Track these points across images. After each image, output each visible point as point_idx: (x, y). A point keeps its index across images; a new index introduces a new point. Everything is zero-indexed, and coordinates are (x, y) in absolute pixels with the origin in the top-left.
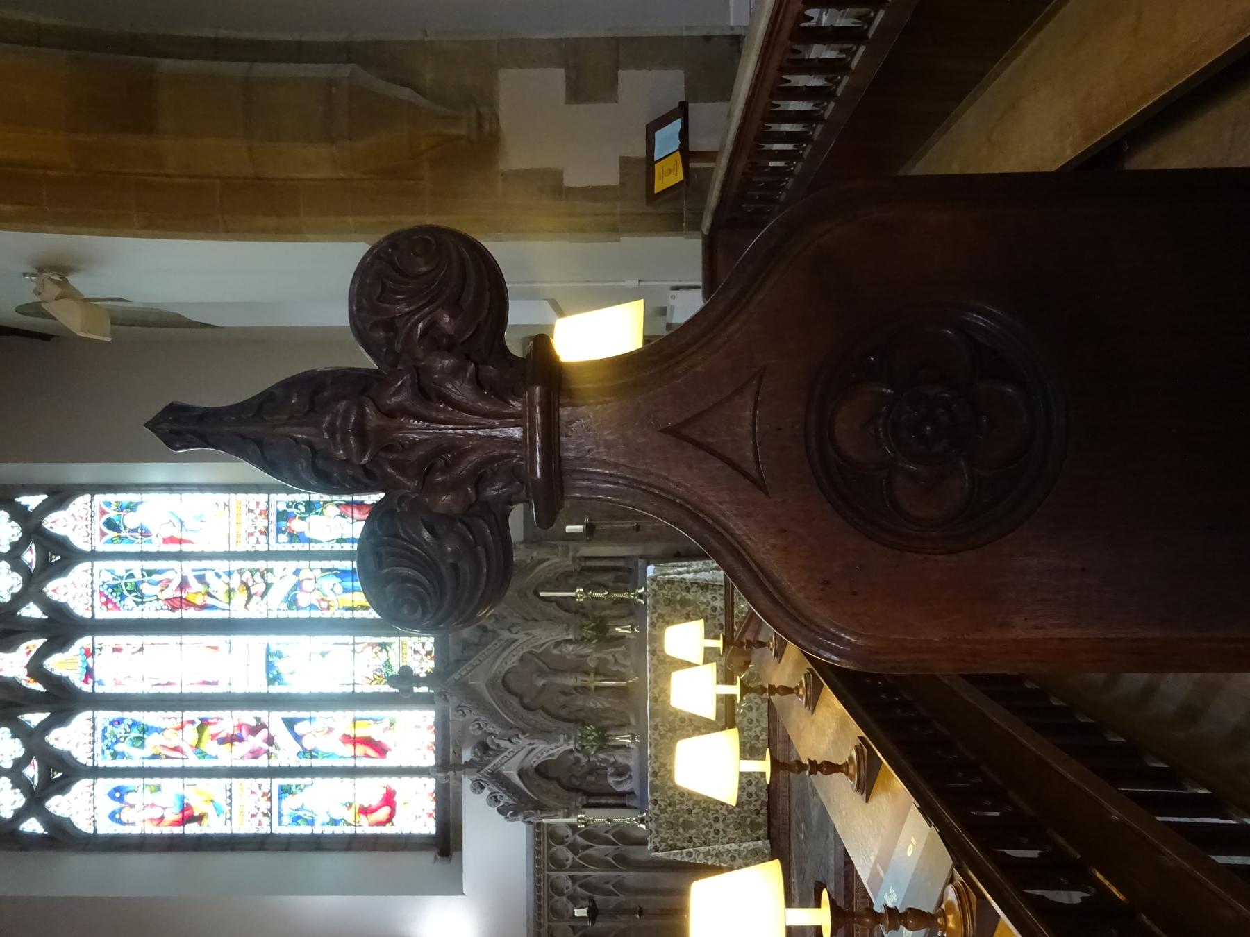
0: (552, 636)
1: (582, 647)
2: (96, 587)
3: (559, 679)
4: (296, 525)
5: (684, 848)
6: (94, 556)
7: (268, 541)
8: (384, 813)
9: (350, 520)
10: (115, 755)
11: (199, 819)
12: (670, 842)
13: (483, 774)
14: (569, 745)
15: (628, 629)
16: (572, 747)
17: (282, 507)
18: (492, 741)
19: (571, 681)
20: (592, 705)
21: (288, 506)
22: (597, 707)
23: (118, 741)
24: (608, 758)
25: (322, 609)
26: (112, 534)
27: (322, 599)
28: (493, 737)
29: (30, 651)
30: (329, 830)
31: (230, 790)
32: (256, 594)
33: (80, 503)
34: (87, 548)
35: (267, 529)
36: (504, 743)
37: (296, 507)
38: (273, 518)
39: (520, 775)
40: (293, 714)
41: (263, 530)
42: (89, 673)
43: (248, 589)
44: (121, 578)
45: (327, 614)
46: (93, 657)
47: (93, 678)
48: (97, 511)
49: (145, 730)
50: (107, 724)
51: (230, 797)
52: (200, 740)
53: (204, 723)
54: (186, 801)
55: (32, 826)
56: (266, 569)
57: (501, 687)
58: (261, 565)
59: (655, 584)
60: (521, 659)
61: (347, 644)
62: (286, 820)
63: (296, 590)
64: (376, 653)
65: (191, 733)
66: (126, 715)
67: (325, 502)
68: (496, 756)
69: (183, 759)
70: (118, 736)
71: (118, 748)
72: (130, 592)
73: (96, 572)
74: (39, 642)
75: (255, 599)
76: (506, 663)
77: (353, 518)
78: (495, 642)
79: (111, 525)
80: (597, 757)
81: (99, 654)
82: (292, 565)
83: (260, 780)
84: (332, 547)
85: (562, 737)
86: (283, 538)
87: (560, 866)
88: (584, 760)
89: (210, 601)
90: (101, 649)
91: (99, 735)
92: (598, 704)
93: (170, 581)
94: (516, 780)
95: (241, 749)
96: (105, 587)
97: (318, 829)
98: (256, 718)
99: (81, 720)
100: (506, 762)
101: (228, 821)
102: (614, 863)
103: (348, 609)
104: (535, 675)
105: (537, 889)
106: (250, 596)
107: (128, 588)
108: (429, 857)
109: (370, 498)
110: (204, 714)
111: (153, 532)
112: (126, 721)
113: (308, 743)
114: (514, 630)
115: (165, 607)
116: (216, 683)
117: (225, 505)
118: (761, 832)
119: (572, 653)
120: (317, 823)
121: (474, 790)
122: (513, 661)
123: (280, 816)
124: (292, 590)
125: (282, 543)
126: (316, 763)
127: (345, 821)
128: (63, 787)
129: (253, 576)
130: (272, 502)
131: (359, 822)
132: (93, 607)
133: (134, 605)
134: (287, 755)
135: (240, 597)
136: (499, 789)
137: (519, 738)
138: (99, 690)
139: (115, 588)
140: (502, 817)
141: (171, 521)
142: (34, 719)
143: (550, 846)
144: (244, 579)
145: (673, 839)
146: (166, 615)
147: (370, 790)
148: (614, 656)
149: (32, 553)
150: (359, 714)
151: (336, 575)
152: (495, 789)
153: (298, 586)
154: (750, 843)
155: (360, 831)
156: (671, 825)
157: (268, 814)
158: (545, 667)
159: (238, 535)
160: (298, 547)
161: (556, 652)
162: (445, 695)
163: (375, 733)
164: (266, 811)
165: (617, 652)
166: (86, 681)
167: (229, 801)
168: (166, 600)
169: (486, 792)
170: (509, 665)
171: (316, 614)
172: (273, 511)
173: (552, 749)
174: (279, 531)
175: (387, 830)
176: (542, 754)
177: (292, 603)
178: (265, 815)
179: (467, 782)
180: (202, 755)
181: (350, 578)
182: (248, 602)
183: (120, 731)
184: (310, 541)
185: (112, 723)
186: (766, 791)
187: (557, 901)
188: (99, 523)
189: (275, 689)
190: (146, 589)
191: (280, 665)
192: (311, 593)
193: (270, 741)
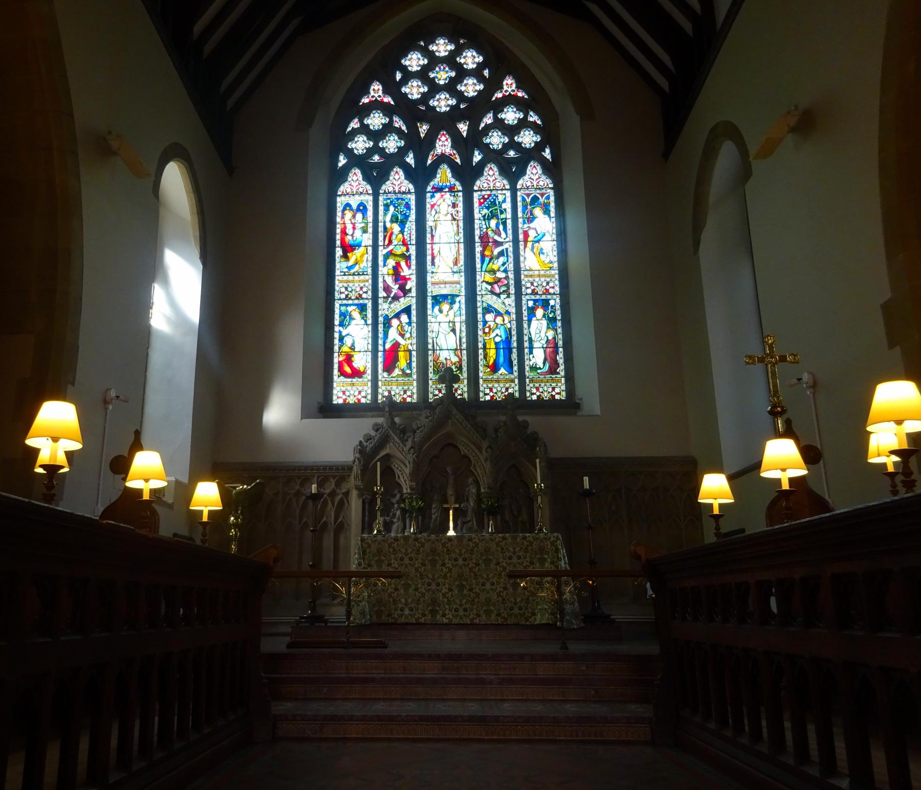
1: (475, 498)
2: (494, 192)
4: (540, 312)
5: (363, 561)
6: (514, 191)
7: (528, 294)
8: (347, 369)
9: (545, 346)
10: (387, 207)
11: (345, 257)
12: (368, 550)
13: (387, 429)
14: (407, 489)
16: (405, 491)
17: (552, 303)
18: (410, 437)
19: (450, 492)
20: (434, 506)
21: (552, 307)
22: (433, 509)
23: (396, 207)
24: (397, 517)
25: (484, 330)
26: (528, 200)
27: (490, 329)
29: (452, 156)
30: (336, 335)
31: (363, 274)
32: (492, 287)
33: (546, 181)
34: (518, 187)
35: (537, 294)
37: (551, 312)
38: (544, 297)
39: (387, 455)
40: (414, 313)
41: (536, 291)
42: (439, 189)
43: (496, 283)
44: (501, 206)
45: (480, 333)
46: (448, 192)
47: (436, 192)
48: (544, 191)
49: (402, 224)
50: (406, 200)
51: (359, 274)
52: (395, 255)
53: (407, 258)
54: (357, 248)
55: (342, 161)
56: (509, 294)
58: (512, 290)
59: (555, 539)
60: (466, 457)
61: (461, 345)
62: (343, 309)
63: (496, 312)
64: (455, 364)
65: (401, 250)
66: (413, 212)
67: (556, 330)
68: (400, 439)
69: (384, 245)
70: (398, 207)
71: (392, 208)
72: (491, 212)
73: (504, 192)
74: (458, 161)
75: (489, 287)
77: (547, 348)
80: (397, 510)
81: (451, 195)
83: (370, 293)
84: (526, 335)
85: (413, 484)
86: (531, 304)
88: (394, 501)
89: (487, 259)
90: (454, 196)
91: (399, 196)
92: (435, 511)
93: (499, 235)
94: (383, 453)
95: (390, 281)
96: (495, 197)
97: (337, 329)
98: (411, 289)
100: (395, 446)
101: (343, 274)
102: (322, 521)
103: (485, 345)
107: (494, 210)
108: (319, 398)
109: (561, 358)
110: (413, 257)
111: (532, 225)
112: (408, 211)
113: (395, 322)
114: (489, 450)
115: (482, 233)
116: (433, 264)
117: (551, 268)
118: (375, 617)
119: (470, 492)
120: (341, 329)
121: (376, 424)
122: (464, 450)
123: (347, 305)
124: (496, 310)
126: (381, 328)
127: (343, 345)
128: (367, 177)
129: (504, 285)
130: (555, 297)
131: (341, 354)
132: (481, 190)
133: (483, 215)
134: (385, 308)
135: (489, 278)
136: (377, 442)
137: (413, 454)
138: (428, 195)
139: (494, 203)
140: (358, 443)
141: (539, 235)
142: (410, 159)
143: (334, 477)
144: (502, 280)
145: (370, 552)
146: (477, 232)
148: (470, 521)
149: (514, 155)
150: (414, 353)
151: (507, 338)
152: (376, 439)
153: (498, 314)
154: (368, 610)
155: (336, 355)
156: (379, 551)
157: (347, 298)
159: (531, 276)
160: (525, 313)
161: (470, 480)
162: (441, 404)
163: (402, 363)
164: (349, 296)
165: (473, 523)
166: (433, 188)
167: (356, 274)
168: (487, 233)
169: (373, 433)
170: (460, 447)
171: (480, 326)
172: (549, 297)
173: (403, 478)
174: (535, 301)
175: (336, 372)
176: (400, 471)
178: (347, 296)
179: (380, 420)
180: (386, 257)
181: (505, 347)
182: (487, 283)
183: (402, 208)
184: (530, 321)
185: (407, 203)
186: (405, 621)
187: (296, 482)
188: (537, 193)
190: (493, 223)
192: (495, 321)
193: (396, 298)
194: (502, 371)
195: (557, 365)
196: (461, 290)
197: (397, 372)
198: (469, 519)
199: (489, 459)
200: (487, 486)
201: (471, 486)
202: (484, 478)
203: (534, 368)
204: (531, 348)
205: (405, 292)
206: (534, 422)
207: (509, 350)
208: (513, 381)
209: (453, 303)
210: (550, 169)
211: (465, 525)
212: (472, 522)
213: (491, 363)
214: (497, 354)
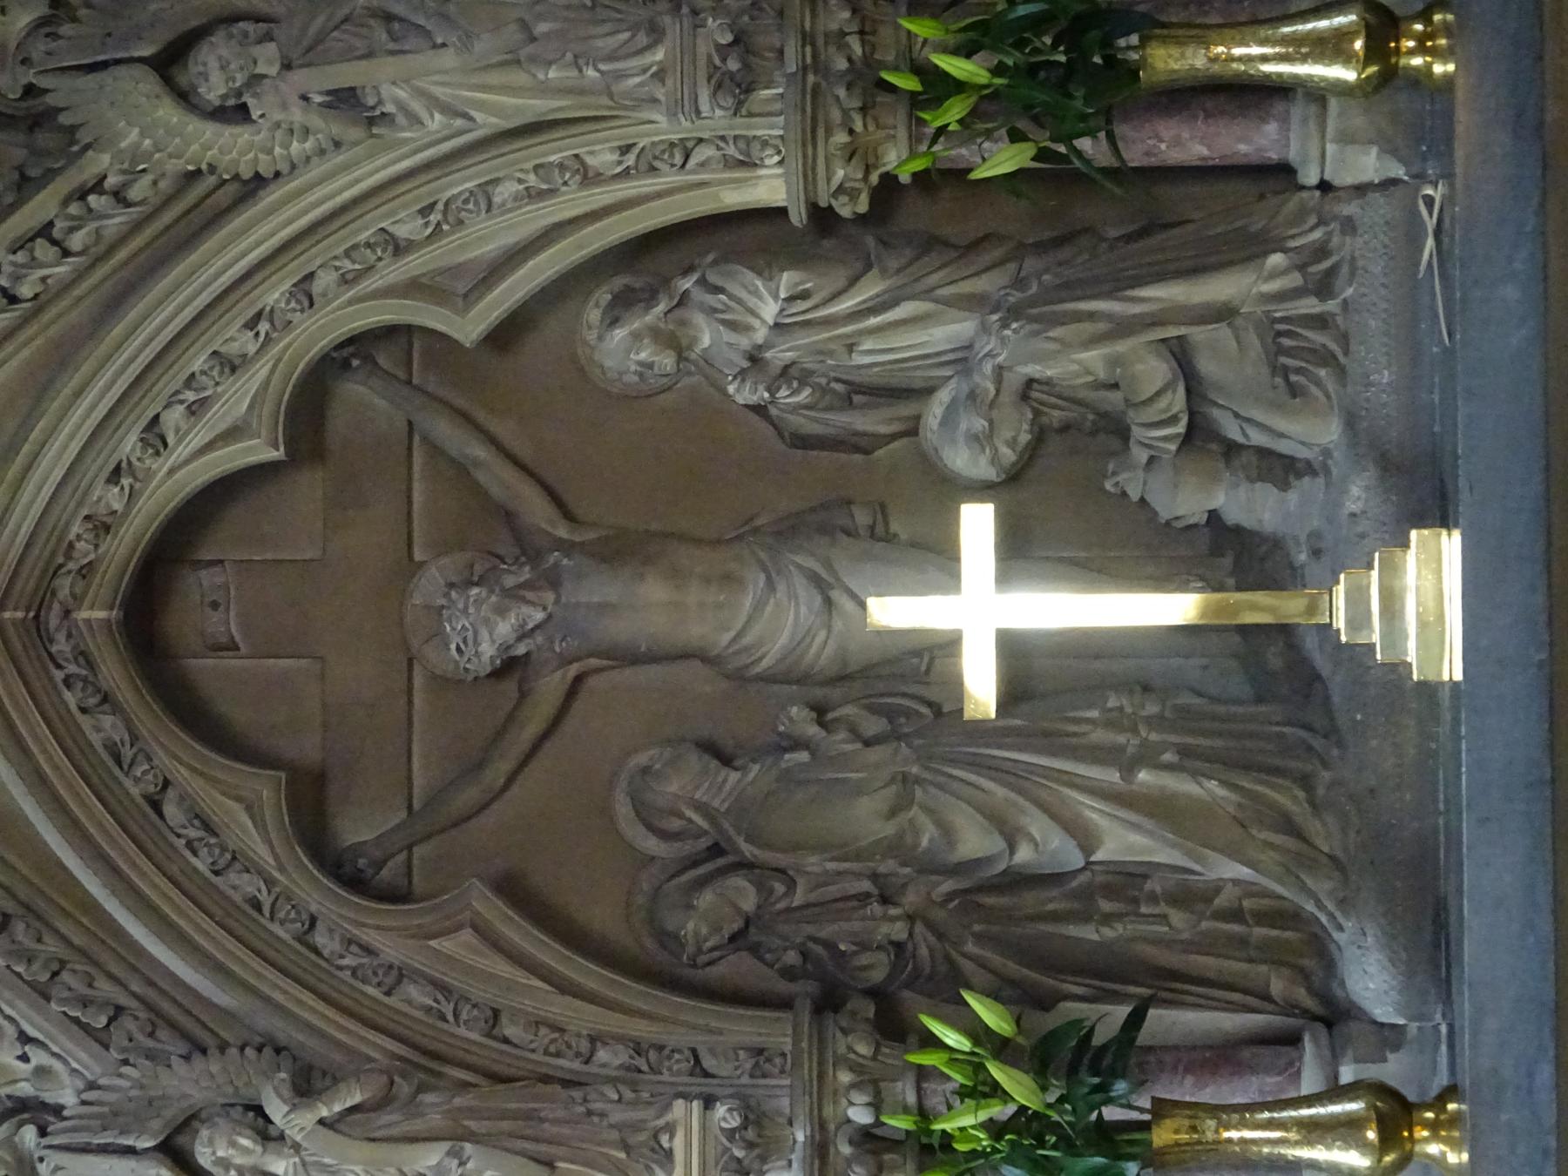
0: (589, 178)
3: (655, 590)
15: (1330, 47)
20: (975, 841)
22: (1024, 854)
28: (29, 1135)
57: (114, 672)
76: (155, 439)
78: (43, 206)
92: (1037, 825)
104: (429, 585)
119: (779, 355)
137: (267, 1135)
148: (1181, 355)
158: (536, 510)
165: (1223, 313)
198: (1154, 371)
199: (345, 75)
200: (716, 117)
201: (706, 337)
202: (603, 158)
211: (1233, 432)
212: (1197, 334)
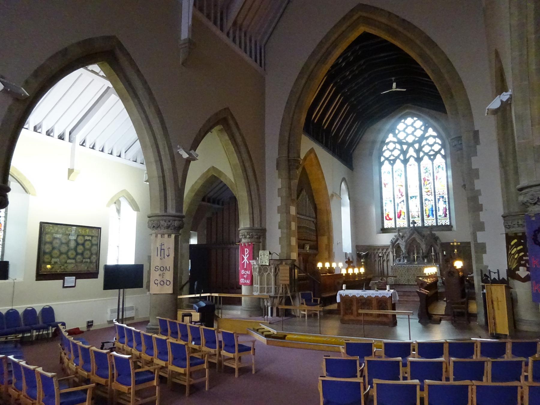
4: (441, 199)
8: (388, 218)
17: (444, 197)
26: (437, 167)
33: (443, 161)
36: (404, 240)
45: (424, 206)
55: (382, 159)
58: (433, 194)
75: (426, 193)
79: (439, 166)
82: (433, 199)
86: (439, 197)
87: (382, 250)
89: (425, 185)
99: (402, 165)
105: (378, 247)
106: (427, 192)
108: (381, 227)
113: (400, 204)
122: (418, 241)
125: (437, 197)
135: (427, 190)
139: (427, 168)
147: (392, 216)
150: (406, 213)
153: (429, 201)
163: (402, 216)
169: (395, 237)
171: (424, 204)
174: (440, 196)
177: (426, 200)
179: (396, 234)
184: (438, 202)
189: (409, 198)
191: (414, 199)
193: (400, 198)
194: (431, 217)
195: (447, 215)
196: (418, 194)
197: (401, 218)
203: (440, 216)
204: (439, 210)
205: (402, 196)
206: (437, 233)
207: (433, 211)
208: (434, 220)
209: (416, 198)
210: (444, 157)
213: (427, 215)
214: (429, 212)
